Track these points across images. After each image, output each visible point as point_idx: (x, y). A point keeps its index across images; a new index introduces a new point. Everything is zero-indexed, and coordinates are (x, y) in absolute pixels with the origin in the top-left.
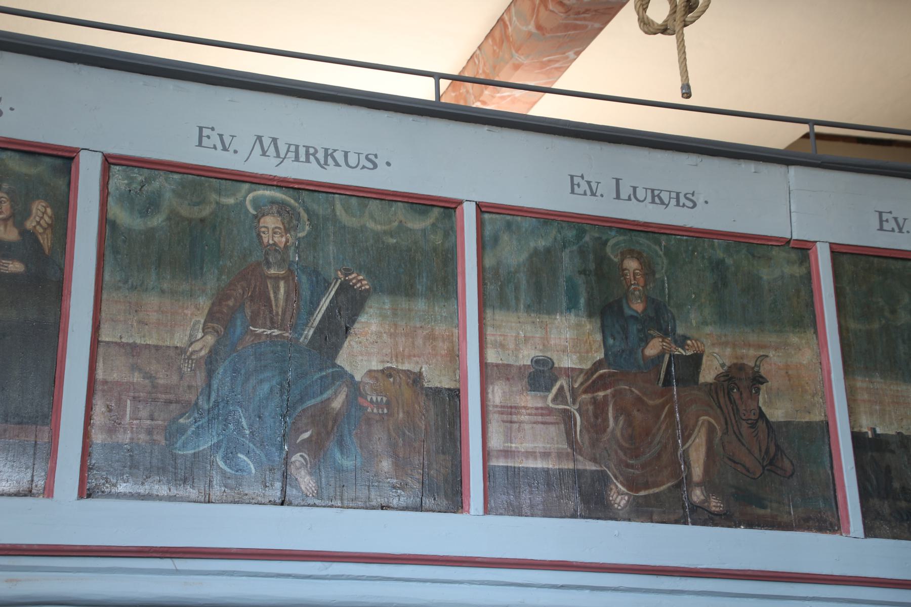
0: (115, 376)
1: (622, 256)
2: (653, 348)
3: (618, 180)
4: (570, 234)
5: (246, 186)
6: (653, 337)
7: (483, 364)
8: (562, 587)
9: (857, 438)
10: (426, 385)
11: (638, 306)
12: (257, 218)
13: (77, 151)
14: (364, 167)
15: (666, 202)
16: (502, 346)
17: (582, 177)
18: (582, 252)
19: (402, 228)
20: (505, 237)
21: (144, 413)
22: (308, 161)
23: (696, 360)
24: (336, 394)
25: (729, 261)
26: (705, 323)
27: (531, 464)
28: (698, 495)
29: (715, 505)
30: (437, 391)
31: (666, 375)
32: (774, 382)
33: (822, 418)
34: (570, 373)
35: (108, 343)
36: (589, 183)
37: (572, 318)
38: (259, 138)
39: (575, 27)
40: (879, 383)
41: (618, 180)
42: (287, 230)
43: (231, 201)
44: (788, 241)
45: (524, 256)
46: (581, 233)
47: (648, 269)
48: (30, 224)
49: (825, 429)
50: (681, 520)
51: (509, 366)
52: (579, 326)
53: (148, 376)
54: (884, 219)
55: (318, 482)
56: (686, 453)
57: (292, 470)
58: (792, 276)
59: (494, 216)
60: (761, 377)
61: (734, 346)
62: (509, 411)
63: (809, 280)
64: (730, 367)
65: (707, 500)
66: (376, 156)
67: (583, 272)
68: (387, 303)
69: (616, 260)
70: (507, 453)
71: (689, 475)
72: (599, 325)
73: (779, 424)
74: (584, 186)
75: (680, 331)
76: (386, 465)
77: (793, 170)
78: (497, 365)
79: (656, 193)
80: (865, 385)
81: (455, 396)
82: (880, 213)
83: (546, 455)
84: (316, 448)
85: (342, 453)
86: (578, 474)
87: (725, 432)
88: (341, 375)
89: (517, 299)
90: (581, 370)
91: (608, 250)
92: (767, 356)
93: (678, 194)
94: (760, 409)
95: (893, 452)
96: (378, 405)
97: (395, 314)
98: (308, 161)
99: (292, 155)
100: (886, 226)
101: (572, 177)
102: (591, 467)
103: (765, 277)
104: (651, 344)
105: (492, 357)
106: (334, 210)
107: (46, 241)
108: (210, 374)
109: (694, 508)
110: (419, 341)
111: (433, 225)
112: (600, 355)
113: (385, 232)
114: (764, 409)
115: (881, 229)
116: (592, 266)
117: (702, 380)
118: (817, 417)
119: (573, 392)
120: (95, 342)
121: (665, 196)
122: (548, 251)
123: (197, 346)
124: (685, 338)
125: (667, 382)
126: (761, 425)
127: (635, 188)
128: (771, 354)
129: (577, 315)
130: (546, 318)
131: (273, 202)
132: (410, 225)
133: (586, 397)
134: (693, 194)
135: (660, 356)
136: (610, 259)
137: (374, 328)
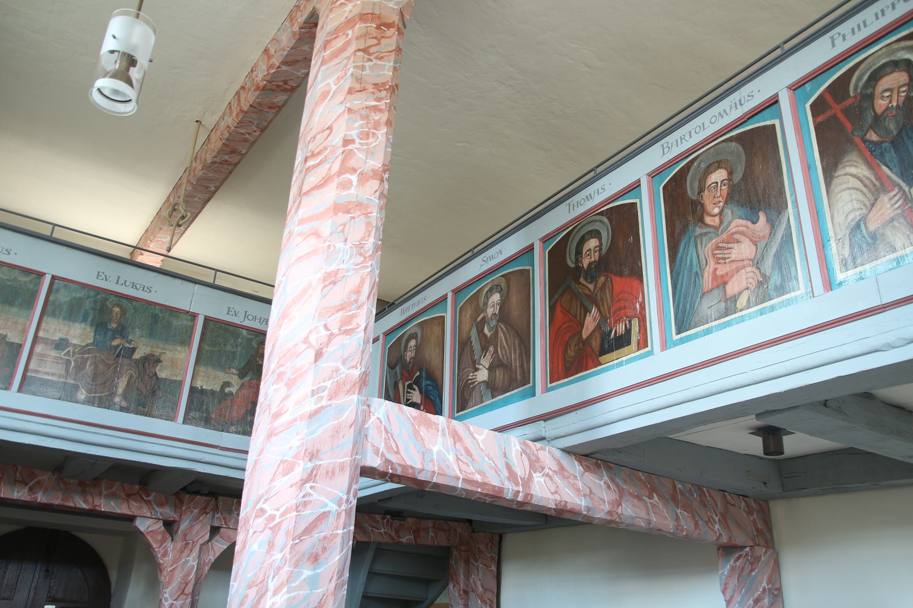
1: (114, 306)
3: (119, 277)
4: (92, 293)
6: (117, 338)
8: (45, 424)
9: (193, 389)
10: (7, 340)
14: (4, 253)
15: (138, 288)
17: (103, 273)
18: (95, 302)
19: (15, 279)
23: (133, 350)
26: (142, 336)
27: (46, 377)
30: (12, 343)
31: (118, 354)
32: (164, 363)
33: (181, 379)
34: (75, 346)
36: (106, 276)
37: (83, 325)
40: (210, 370)
41: (119, 277)
45: (69, 298)
46: (98, 294)
47: (124, 312)
49: (181, 384)
52: (85, 329)
54: (230, 310)
59: (59, 281)
60: (160, 360)
61: (152, 347)
63: (192, 329)
64: (148, 355)
67: (94, 309)
69: (110, 307)
72: (94, 329)
75: (130, 338)
77: (197, 285)
78: (43, 338)
79: (135, 284)
80: (204, 370)
82: (229, 308)
83: (53, 375)
89: (60, 314)
90: (80, 346)
93: (144, 286)
94: (156, 372)
95: (207, 396)
100: (230, 313)
103: (174, 324)
104: (115, 340)
110: (10, 323)
113: (7, 280)
114: (157, 372)
115: (228, 314)
116: (98, 307)
117: (133, 357)
118: (179, 378)
121: (138, 286)
122: (80, 298)
124: (131, 341)
128: (168, 352)
129: (85, 324)
130: (71, 323)
132: (19, 279)
134: (151, 288)
135: (118, 346)
136: (107, 306)
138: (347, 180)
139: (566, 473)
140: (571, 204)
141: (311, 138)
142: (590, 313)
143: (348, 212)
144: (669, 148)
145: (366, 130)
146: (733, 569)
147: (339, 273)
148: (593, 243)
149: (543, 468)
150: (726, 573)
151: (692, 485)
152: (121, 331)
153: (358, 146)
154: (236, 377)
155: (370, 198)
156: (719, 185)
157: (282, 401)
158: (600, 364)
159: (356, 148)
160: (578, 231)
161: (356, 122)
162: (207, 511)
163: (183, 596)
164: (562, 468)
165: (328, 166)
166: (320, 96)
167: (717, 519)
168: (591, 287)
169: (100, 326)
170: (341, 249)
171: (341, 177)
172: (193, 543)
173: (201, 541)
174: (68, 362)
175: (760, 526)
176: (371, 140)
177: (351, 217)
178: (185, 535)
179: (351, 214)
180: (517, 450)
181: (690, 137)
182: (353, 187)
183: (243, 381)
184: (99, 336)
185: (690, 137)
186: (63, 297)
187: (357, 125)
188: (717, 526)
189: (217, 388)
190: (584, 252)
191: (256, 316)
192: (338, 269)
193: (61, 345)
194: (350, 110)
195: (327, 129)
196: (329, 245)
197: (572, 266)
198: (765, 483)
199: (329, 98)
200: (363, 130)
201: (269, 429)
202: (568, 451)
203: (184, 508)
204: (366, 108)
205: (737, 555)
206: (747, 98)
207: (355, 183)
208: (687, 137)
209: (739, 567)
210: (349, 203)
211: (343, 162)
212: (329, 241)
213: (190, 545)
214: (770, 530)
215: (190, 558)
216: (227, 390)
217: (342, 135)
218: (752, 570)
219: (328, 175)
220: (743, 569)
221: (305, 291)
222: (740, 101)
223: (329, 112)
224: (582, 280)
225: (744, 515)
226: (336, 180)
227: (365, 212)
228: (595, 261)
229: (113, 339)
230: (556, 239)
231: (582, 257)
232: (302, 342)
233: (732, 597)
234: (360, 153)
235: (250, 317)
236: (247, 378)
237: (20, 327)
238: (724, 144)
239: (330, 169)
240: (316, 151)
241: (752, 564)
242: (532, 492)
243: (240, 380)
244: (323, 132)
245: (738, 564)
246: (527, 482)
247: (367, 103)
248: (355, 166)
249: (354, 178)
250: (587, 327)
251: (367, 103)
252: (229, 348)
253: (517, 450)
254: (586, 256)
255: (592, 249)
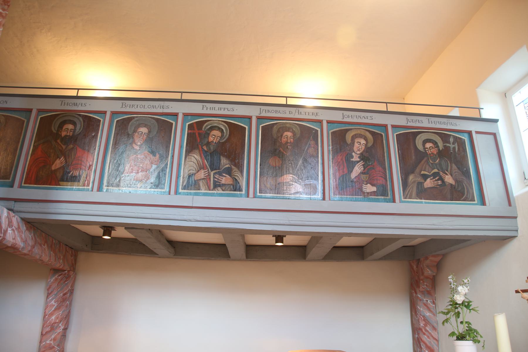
139: (20, 230)
140: (63, 102)
142: (60, 159)
144: (126, 106)
146: (56, 279)
148: (70, 127)
149: (12, 226)
150: (52, 281)
151: (58, 241)
156: (143, 134)
158: (60, 185)
160: (63, 116)
164: (19, 227)
167: (62, 257)
168: (64, 147)
175: (73, 262)
180: (5, 216)
181: (137, 107)
185: (137, 107)
188: (61, 261)
190: (64, 128)
197: (54, 131)
198: (87, 245)
202: (23, 219)
205: (60, 274)
206: (166, 107)
208: (136, 106)
209: (60, 279)
214: (76, 264)
218: (66, 281)
220: (62, 279)
222: (163, 106)
224: (59, 141)
225: (70, 256)
228: (69, 136)
230: (47, 114)
231: (62, 130)
233: (52, 292)
238: (150, 119)
241: (67, 278)
242: (6, 238)
245: (59, 277)
246: (6, 232)
250: (56, 165)
253: (5, 216)
254: (64, 131)
255: (70, 129)
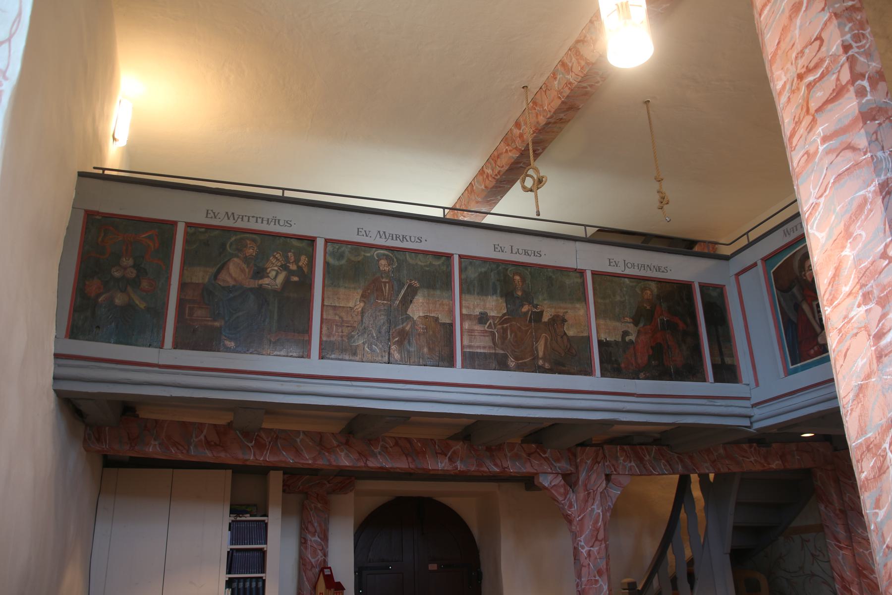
0: (329, 317)
1: (514, 275)
2: (525, 308)
3: (512, 246)
4: (494, 266)
5: (374, 249)
7: (461, 314)
9: (600, 343)
10: (440, 322)
11: (520, 293)
12: (378, 261)
13: (316, 238)
14: (417, 242)
16: (468, 307)
17: (498, 245)
20: (470, 267)
21: (340, 330)
22: (396, 240)
23: (541, 313)
24: (407, 324)
25: (554, 277)
26: (544, 300)
27: (479, 351)
28: (541, 362)
29: (547, 366)
30: (444, 324)
31: (530, 319)
33: (587, 335)
34: (493, 317)
35: (327, 305)
36: (501, 247)
37: (495, 298)
38: (379, 232)
39: (500, 187)
41: (512, 246)
42: (389, 265)
43: (368, 255)
44: (576, 270)
45: (477, 275)
46: (498, 266)
47: (523, 280)
48: (300, 264)
49: (589, 339)
50: (535, 371)
51: (471, 315)
52: (497, 300)
53: (340, 317)
55: (401, 356)
56: (536, 348)
57: (392, 351)
58: (577, 282)
59: (465, 260)
62: (471, 331)
63: (584, 284)
64: (554, 316)
65: (544, 364)
66: (421, 238)
68: (426, 291)
69: (511, 276)
70: (470, 347)
71: (538, 355)
72: (505, 299)
73: (573, 337)
74: (499, 248)
76: (426, 350)
77: (577, 243)
78: (467, 315)
81: (451, 326)
83: (484, 348)
84: (400, 343)
85: (409, 345)
86: (496, 354)
87: (552, 340)
88: (409, 318)
89: (474, 290)
90: (498, 317)
91: (508, 272)
92: (567, 312)
93: (534, 251)
94: (564, 331)
96: (423, 329)
97: (429, 296)
98: (396, 240)
99: (391, 238)
100: (612, 264)
101: (494, 245)
102: (502, 352)
103: (567, 283)
104: (524, 307)
105: (465, 312)
106: (406, 258)
107: (306, 270)
108: (362, 317)
109: (539, 367)
110: (438, 306)
111: (443, 263)
112: (505, 311)
113: (425, 266)
114: (566, 331)
115: (610, 265)
116: (502, 278)
117: (543, 321)
118: (585, 334)
119: (494, 324)
120: (323, 305)
122: (485, 273)
123: (357, 307)
125: (530, 321)
126: (565, 337)
127: (518, 249)
129: (496, 296)
130: (485, 298)
131: (384, 255)
132: (434, 263)
133: (500, 326)
135: (528, 311)
136: (509, 276)
137: (421, 301)
138: (860, 87)
141: (798, 54)
143: (874, 119)
145: (856, 32)
147: (889, 182)
152: (528, 298)
153: (856, 50)
154: (632, 325)
155: (885, 100)
157: (879, 321)
159: (856, 53)
161: (845, 25)
162: (599, 460)
163: (597, 543)
165: (834, 77)
166: (791, 10)
169: (508, 295)
170: (882, 157)
171: (855, 85)
172: (594, 491)
173: (600, 490)
174: (493, 334)
176: (864, 42)
177: (878, 124)
178: (586, 486)
179: (877, 120)
182: (869, 94)
183: (638, 328)
184: (510, 305)
186: (472, 274)
187: (847, 29)
189: (619, 339)
191: (634, 264)
192: (887, 179)
193: (483, 318)
194: (836, 15)
195: (816, 39)
196: (872, 156)
199: (804, 8)
200: (854, 32)
201: (876, 350)
203: (578, 460)
204: (847, 9)
207: (868, 89)
210: (872, 109)
211: (852, 69)
212: (870, 152)
213: (592, 494)
215: (595, 507)
216: (627, 339)
217: (839, 42)
219: (839, 86)
221: (861, 207)
223: (810, 23)
226: (852, 89)
227: (887, 116)
229: (522, 306)
232: (880, 258)
234: (860, 56)
235: (629, 265)
236: (641, 325)
237: (446, 308)
239: (838, 79)
240: (812, 65)
243: (636, 327)
244: (811, 44)
247: (845, 4)
248: (863, 71)
249: (865, 83)
251: (845, 4)
252: (618, 298)
